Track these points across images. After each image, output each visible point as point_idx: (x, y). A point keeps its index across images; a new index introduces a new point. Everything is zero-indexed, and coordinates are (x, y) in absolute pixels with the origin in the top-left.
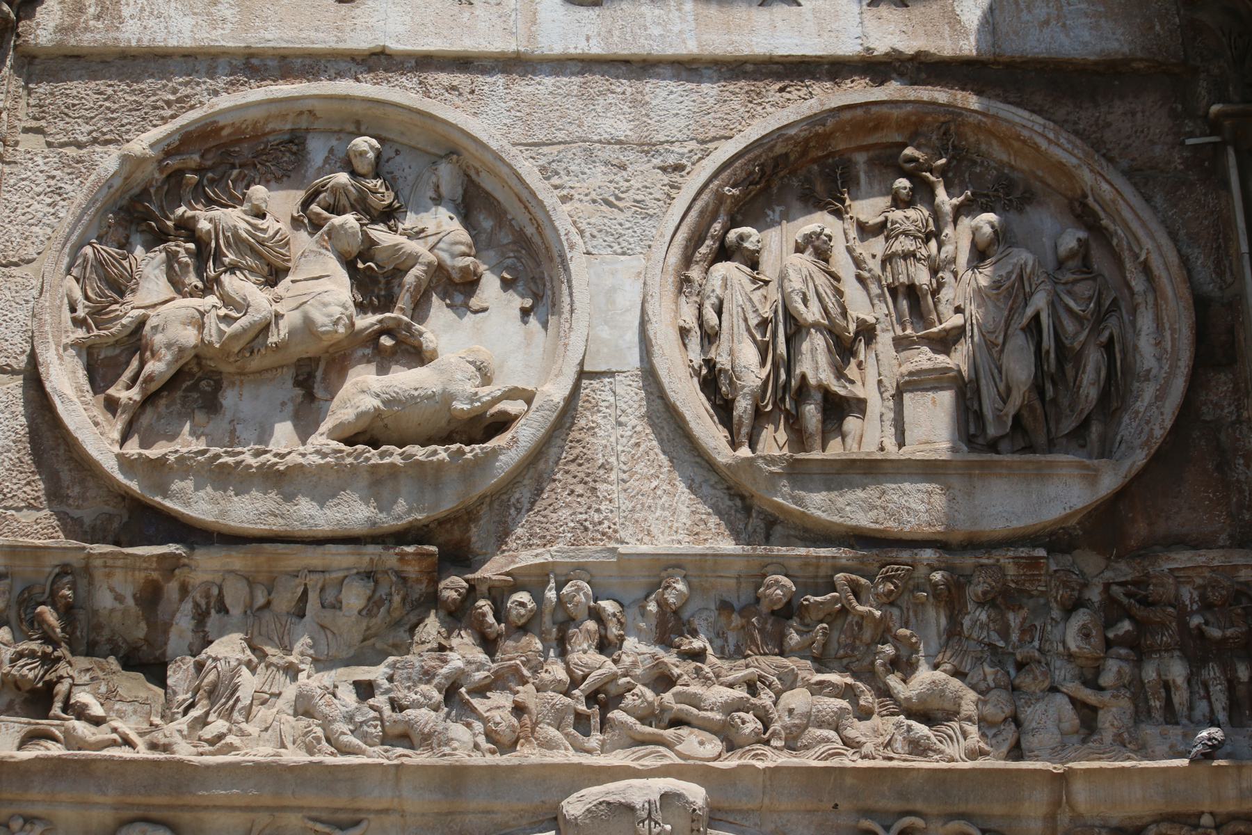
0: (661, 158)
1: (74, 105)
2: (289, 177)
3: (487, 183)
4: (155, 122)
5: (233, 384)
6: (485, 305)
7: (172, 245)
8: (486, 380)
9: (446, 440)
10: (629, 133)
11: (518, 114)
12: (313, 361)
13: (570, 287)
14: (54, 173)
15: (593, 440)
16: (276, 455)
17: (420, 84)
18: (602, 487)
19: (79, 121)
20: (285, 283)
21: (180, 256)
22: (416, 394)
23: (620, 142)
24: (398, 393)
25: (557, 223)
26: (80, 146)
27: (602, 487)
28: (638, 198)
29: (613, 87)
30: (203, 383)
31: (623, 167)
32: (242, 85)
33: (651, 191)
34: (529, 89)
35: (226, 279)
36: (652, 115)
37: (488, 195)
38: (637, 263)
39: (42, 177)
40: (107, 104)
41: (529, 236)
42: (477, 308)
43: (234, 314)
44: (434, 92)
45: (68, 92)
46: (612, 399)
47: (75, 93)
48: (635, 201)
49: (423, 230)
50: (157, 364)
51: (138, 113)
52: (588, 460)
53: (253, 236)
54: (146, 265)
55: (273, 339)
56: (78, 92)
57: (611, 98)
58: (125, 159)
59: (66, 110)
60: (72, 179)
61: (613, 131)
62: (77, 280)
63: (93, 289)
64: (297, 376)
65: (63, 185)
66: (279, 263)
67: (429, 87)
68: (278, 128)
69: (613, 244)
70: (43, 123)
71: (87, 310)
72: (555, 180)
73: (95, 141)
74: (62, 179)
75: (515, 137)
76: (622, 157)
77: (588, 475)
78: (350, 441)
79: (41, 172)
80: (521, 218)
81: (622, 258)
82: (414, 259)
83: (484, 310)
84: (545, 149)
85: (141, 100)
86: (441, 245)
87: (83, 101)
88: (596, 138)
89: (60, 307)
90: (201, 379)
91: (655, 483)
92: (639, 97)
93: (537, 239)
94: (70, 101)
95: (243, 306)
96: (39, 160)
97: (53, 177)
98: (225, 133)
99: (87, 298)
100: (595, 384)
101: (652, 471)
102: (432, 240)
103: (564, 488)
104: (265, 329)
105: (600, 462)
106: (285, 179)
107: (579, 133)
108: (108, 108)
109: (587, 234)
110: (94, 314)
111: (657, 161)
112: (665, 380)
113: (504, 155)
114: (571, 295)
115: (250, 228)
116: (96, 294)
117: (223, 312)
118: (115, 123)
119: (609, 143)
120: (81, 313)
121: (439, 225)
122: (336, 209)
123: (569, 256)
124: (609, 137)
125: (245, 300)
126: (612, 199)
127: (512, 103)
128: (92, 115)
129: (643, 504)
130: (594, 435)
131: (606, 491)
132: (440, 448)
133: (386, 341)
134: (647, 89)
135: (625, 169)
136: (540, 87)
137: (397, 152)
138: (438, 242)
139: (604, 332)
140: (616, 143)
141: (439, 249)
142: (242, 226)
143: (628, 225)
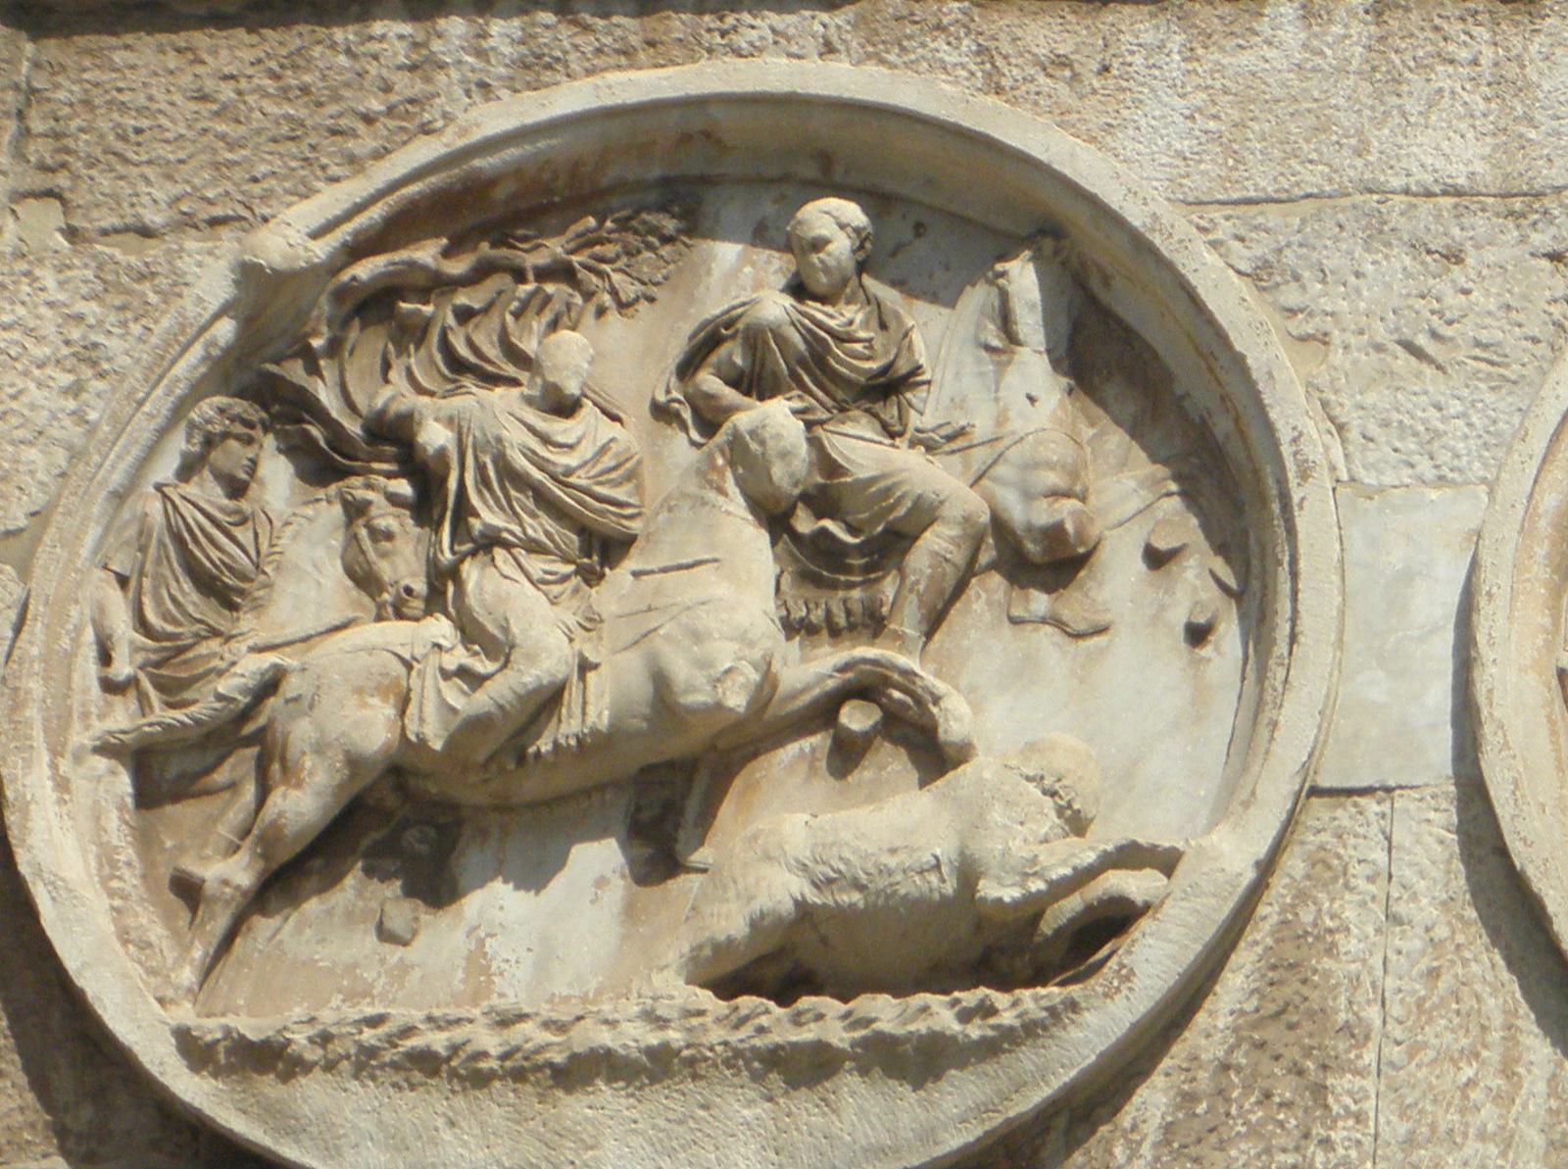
0: (1553, 230)
1: (138, 131)
2: (651, 300)
3: (1129, 305)
4: (334, 170)
5: (483, 833)
6: (1102, 619)
7: (359, 491)
8: (1077, 823)
9: (940, 977)
10: (1479, 167)
11: (1212, 125)
12: (682, 769)
13: (1294, 575)
14: (81, 307)
15: (1327, 963)
16: (547, 1025)
17: (978, 53)
18: (1336, 1082)
19: (148, 170)
20: (619, 577)
21: (374, 511)
22: (892, 862)
23: (1458, 192)
24: (847, 862)
25: (1273, 415)
26: (146, 232)
27: (1336, 1082)
28: (1484, 336)
29: (1451, 47)
30: (411, 836)
31: (1454, 256)
32: (549, 67)
33: (1521, 317)
34: (1246, 59)
35: (471, 571)
36: (1538, 116)
37: (1128, 336)
38: (1466, 509)
39: (49, 323)
40: (222, 128)
41: (1220, 438)
42: (1082, 627)
43: (482, 666)
44: (1010, 74)
45: (124, 97)
46: (1380, 856)
47: (142, 101)
48: (1478, 344)
49: (961, 433)
50: (294, 793)
51: (292, 147)
52: (1311, 1015)
53: (541, 464)
54: (295, 537)
55: (568, 727)
56: (151, 98)
57: (1443, 77)
58: (249, 274)
59: (119, 146)
60: (124, 324)
61: (1440, 164)
62: (123, 581)
63: (158, 602)
64: (638, 809)
65: (101, 339)
66: (609, 521)
67: (1000, 62)
68: (631, 176)
69: (1416, 458)
70: (62, 180)
71: (140, 658)
72: (1291, 296)
73: (187, 223)
74: (101, 322)
75: (1197, 184)
76: (1456, 232)
77: (1307, 1052)
78: (727, 987)
79: (51, 305)
80: (1201, 396)
81: (1434, 495)
82: (925, 514)
83: (1101, 630)
84: (1272, 215)
85: (303, 113)
86: (1001, 470)
87: (164, 121)
88: (1396, 183)
89: (70, 657)
90: (405, 825)
91: (1468, 1072)
92: (1511, 71)
93: (1234, 449)
94: (130, 122)
95: (499, 648)
96: (49, 279)
97: (79, 318)
98: (501, 193)
99: (142, 624)
100: (1344, 814)
101: (1464, 1042)
102: (980, 456)
103: (1248, 1088)
104: (548, 701)
105: (1342, 1017)
106: (643, 306)
107: (1353, 169)
108: (222, 137)
109: (1354, 435)
110: (158, 665)
111: (1542, 239)
112: (1503, 811)
113: (1157, 240)
114: (1295, 592)
115: (534, 444)
116: (167, 617)
117: (458, 657)
118: (238, 174)
119: (1429, 194)
120: (122, 668)
121: (1001, 419)
122: (756, 383)
123: (1296, 499)
124: (1428, 178)
125: (506, 630)
126: (1422, 341)
127: (1200, 98)
128: (182, 155)
129: (1433, 1127)
130: (1331, 950)
131: (1350, 1093)
132: (935, 1000)
133: (856, 718)
134: (1534, 48)
135: (1459, 261)
136: (1270, 53)
137: (919, 229)
138: (995, 462)
139: (1373, 686)
140: (1445, 193)
141: (996, 480)
142: (516, 438)
143: (1456, 407)
